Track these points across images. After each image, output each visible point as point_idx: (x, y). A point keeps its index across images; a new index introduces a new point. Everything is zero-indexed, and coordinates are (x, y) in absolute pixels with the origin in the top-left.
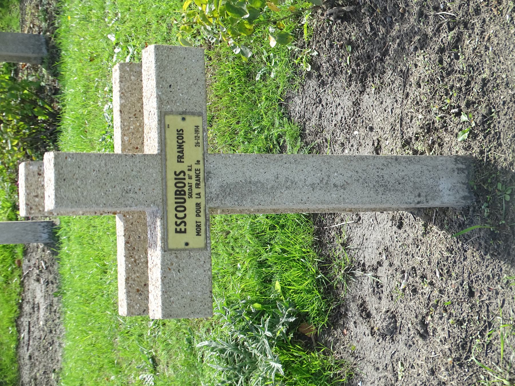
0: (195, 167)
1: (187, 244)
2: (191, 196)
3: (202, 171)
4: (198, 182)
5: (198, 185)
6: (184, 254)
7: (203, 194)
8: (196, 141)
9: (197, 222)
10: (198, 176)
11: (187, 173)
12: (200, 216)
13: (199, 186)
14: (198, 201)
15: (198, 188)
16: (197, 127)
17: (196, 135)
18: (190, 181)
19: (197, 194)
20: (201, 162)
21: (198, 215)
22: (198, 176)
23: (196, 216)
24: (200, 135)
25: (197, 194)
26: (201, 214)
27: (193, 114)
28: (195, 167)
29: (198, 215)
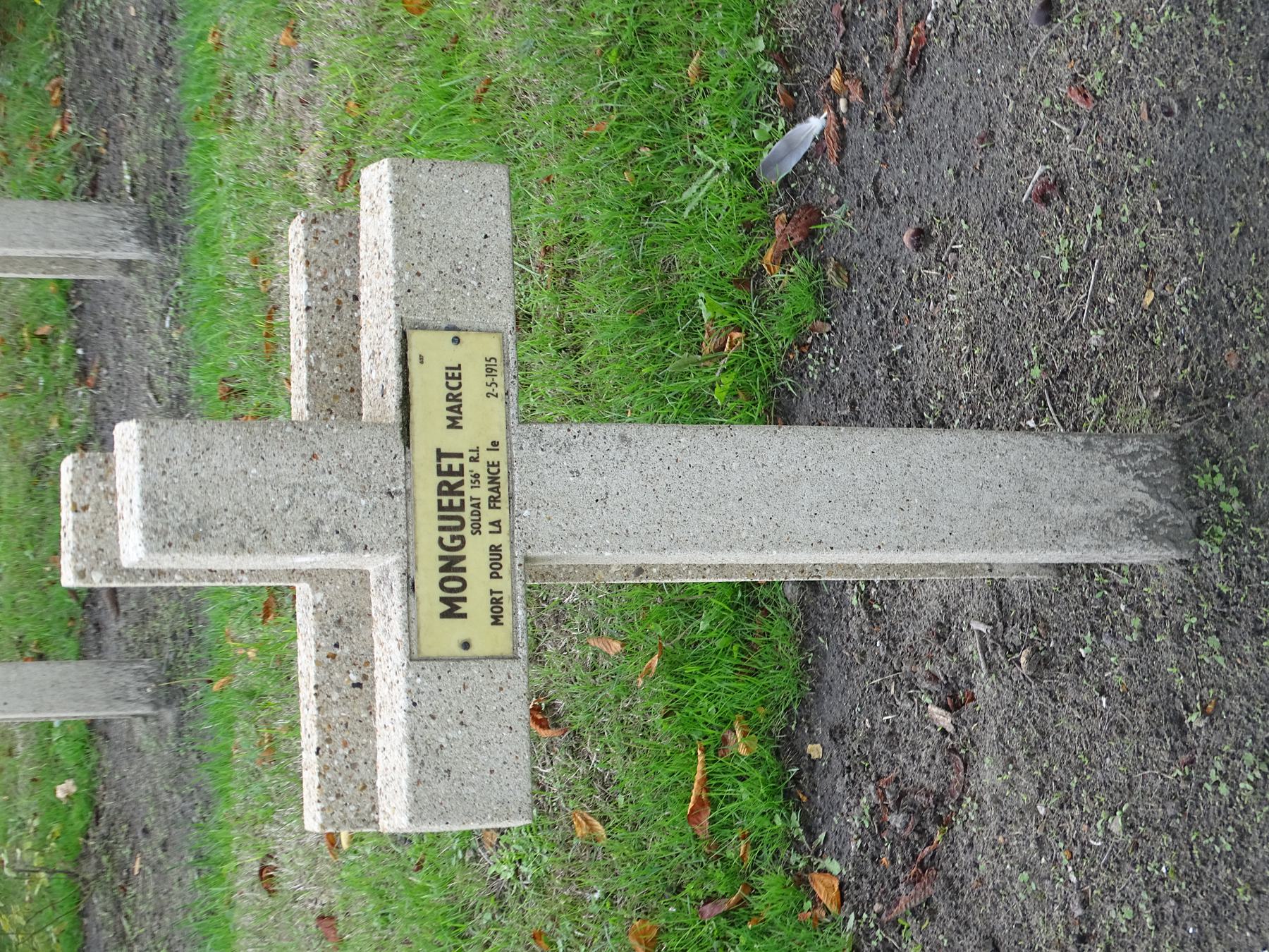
0: (486, 456)
2: (477, 530)
3: (504, 469)
4: (496, 495)
5: (494, 502)
6: (460, 672)
7: (505, 526)
9: (492, 592)
10: (494, 479)
12: (499, 577)
13: (498, 505)
15: (495, 507)
17: (489, 380)
18: (476, 493)
19: (492, 524)
22: (494, 479)
24: (499, 379)
25: (492, 524)
28: (486, 456)
29: (495, 575)
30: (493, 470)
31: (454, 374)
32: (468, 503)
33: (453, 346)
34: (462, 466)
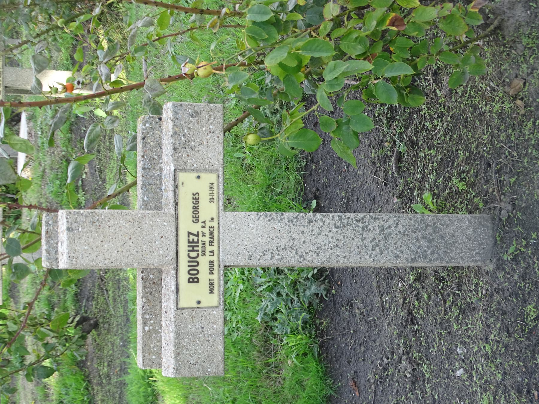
1: (199, 302)
2: (204, 254)
4: (212, 240)
5: (211, 243)
7: (216, 252)
8: (211, 197)
9: (210, 280)
10: (211, 233)
11: (200, 230)
12: (213, 274)
13: (213, 244)
14: (212, 258)
15: (212, 245)
16: (213, 184)
17: (211, 192)
18: (203, 239)
19: (210, 252)
20: (215, 220)
21: (211, 273)
22: (211, 233)
23: (210, 274)
25: (210, 252)
26: (213, 272)
28: (208, 224)
29: (211, 273)
34: (198, 240)
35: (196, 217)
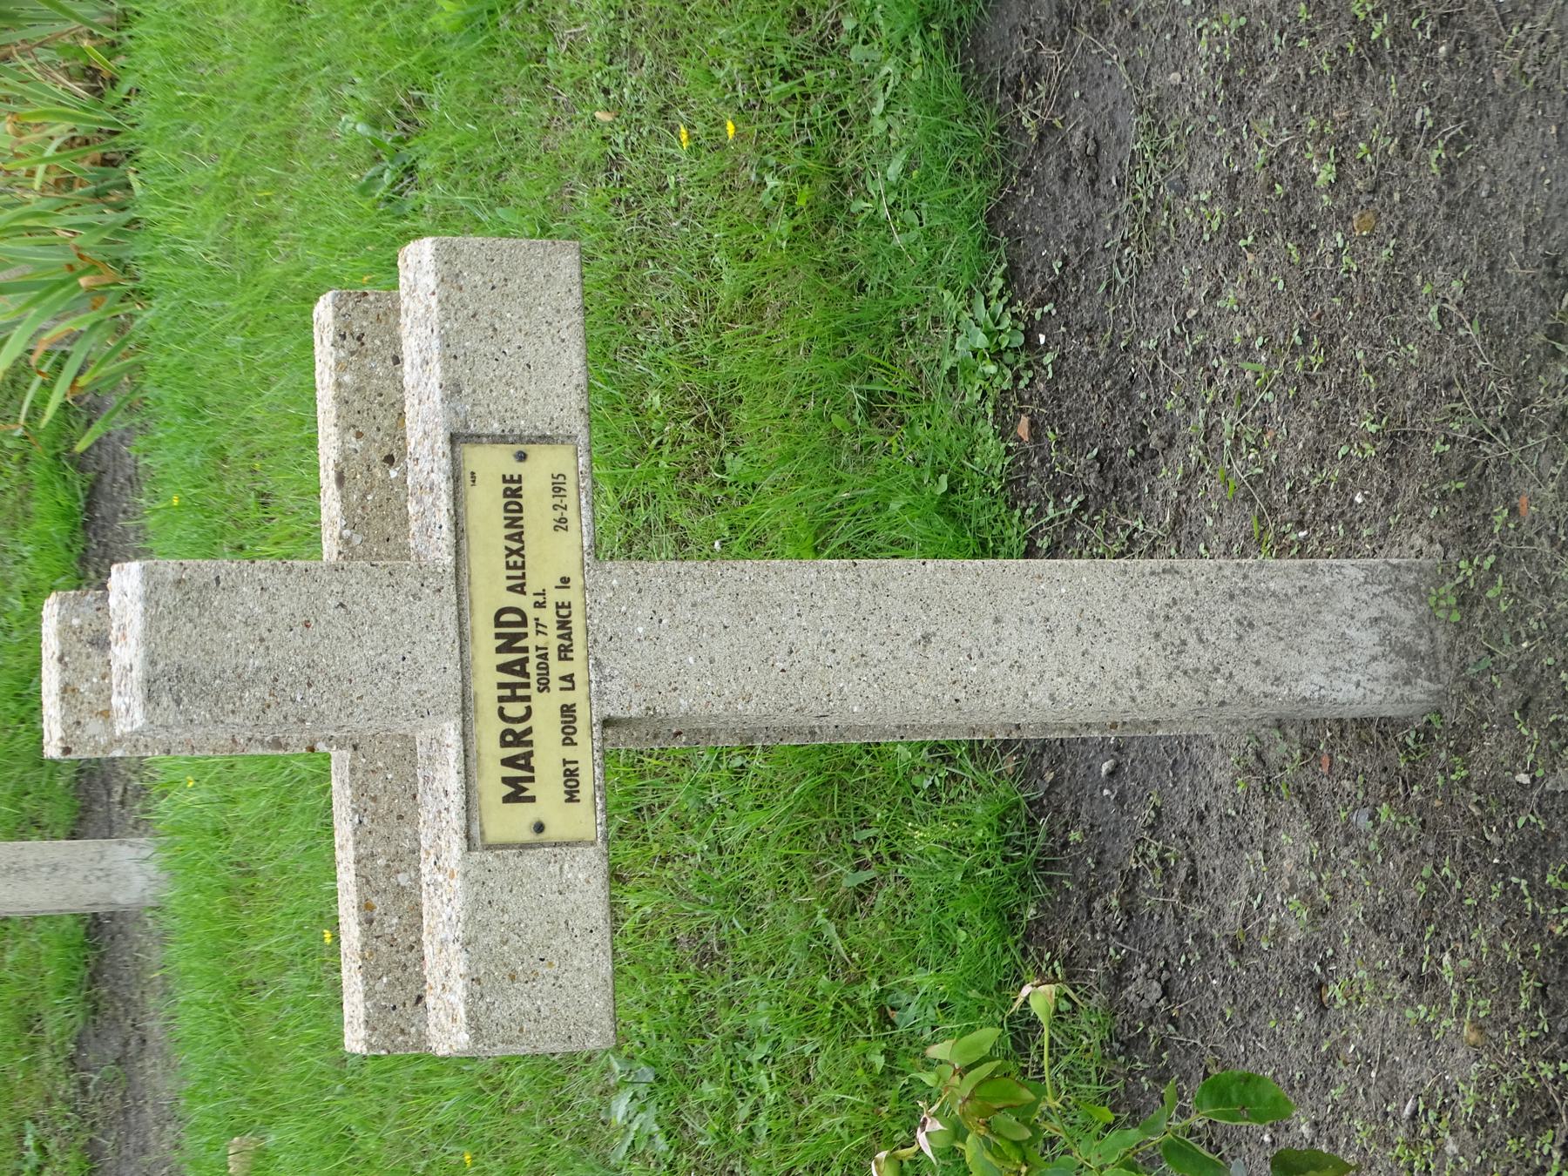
0: (554, 596)
4: (567, 643)
6: (530, 860)
9: (565, 762)
10: (564, 624)
11: (532, 613)
13: (570, 655)
19: (563, 678)
21: (568, 741)
22: (564, 624)
24: (570, 499)
25: (563, 678)
26: (574, 738)
27: (544, 439)
28: (554, 596)
29: (568, 741)
30: (563, 612)
31: (513, 491)
32: (532, 655)
33: (513, 461)
35: (515, 567)
